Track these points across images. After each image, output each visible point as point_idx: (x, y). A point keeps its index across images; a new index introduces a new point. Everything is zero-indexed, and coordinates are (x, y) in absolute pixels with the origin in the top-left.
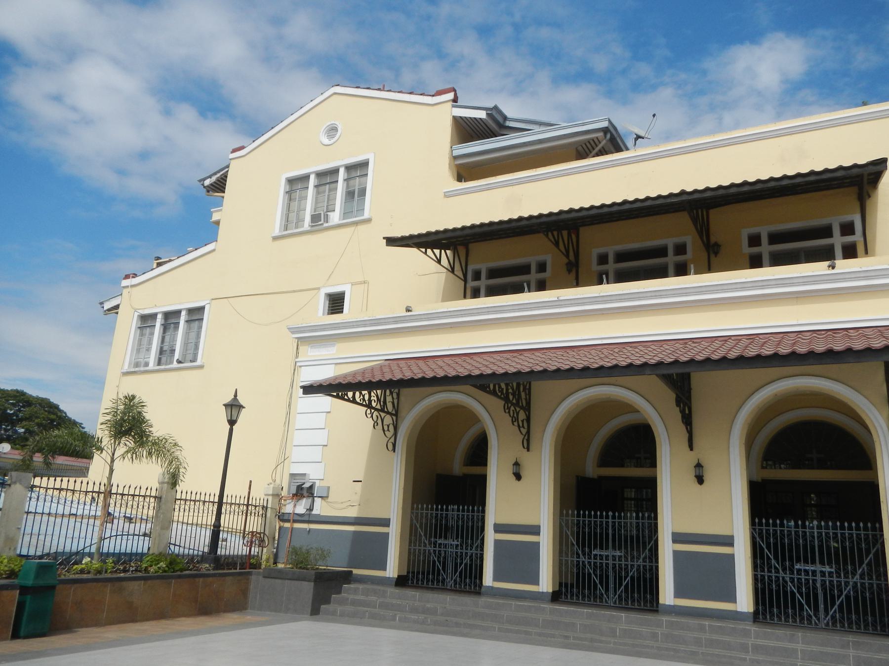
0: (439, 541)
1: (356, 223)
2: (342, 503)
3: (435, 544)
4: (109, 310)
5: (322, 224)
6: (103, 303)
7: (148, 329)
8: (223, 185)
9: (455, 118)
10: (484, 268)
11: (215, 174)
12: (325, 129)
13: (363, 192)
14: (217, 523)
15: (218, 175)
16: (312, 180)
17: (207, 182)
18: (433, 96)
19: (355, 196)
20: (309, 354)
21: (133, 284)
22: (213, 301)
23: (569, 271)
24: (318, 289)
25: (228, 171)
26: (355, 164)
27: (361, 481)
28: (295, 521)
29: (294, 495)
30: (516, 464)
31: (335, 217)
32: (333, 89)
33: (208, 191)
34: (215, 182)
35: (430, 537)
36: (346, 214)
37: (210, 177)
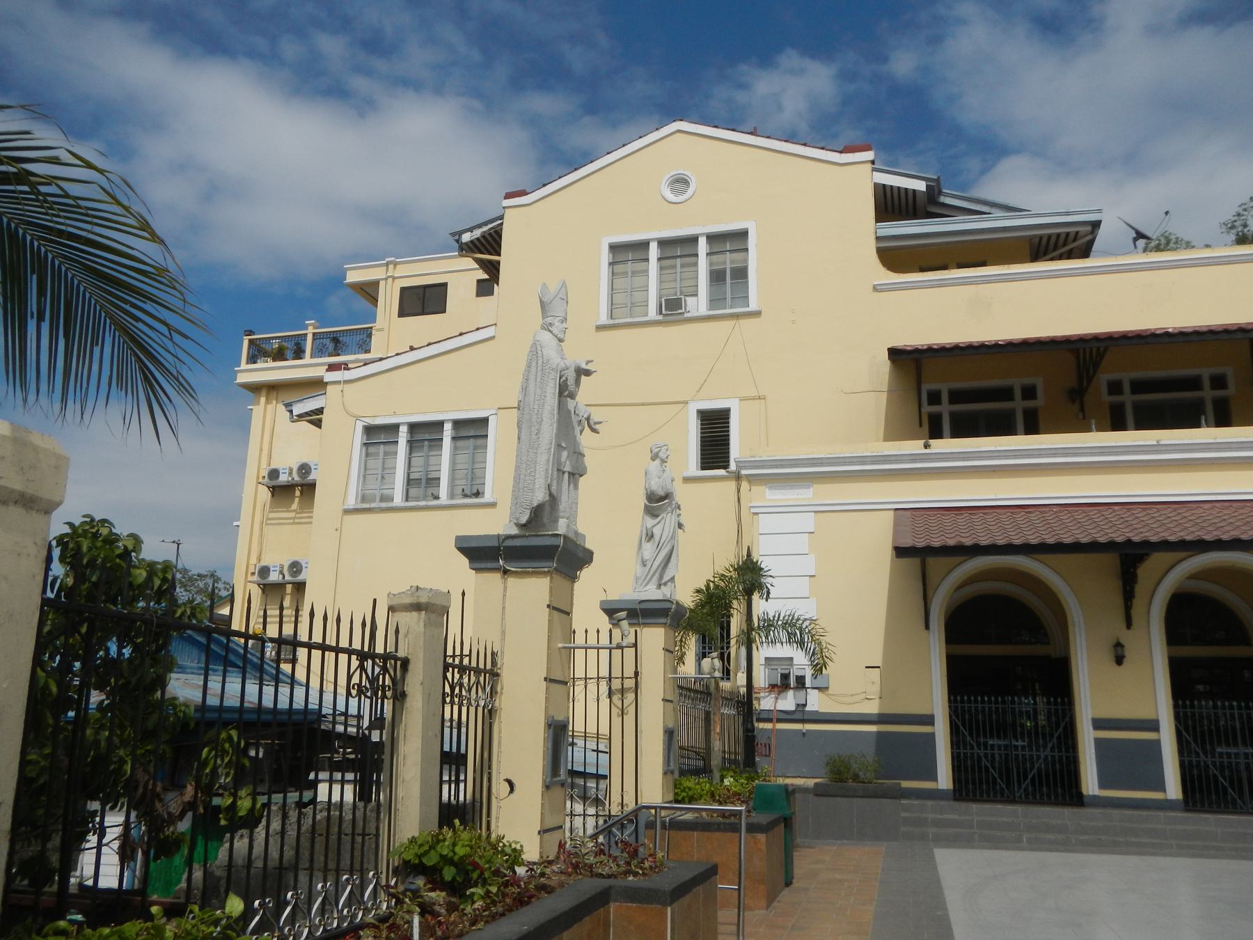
0: (991, 742)
1: (737, 316)
2: (852, 695)
3: (985, 744)
4: (300, 416)
6: (291, 405)
7: (382, 446)
9: (876, 185)
10: (944, 388)
13: (741, 274)
15: (485, 229)
17: (466, 238)
18: (841, 152)
22: (500, 411)
23: (1073, 401)
24: (686, 403)
25: (503, 223)
27: (879, 667)
28: (780, 721)
29: (773, 687)
30: (1118, 645)
31: (699, 304)
34: (478, 239)
35: (978, 735)
36: (714, 301)
37: (471, 230)
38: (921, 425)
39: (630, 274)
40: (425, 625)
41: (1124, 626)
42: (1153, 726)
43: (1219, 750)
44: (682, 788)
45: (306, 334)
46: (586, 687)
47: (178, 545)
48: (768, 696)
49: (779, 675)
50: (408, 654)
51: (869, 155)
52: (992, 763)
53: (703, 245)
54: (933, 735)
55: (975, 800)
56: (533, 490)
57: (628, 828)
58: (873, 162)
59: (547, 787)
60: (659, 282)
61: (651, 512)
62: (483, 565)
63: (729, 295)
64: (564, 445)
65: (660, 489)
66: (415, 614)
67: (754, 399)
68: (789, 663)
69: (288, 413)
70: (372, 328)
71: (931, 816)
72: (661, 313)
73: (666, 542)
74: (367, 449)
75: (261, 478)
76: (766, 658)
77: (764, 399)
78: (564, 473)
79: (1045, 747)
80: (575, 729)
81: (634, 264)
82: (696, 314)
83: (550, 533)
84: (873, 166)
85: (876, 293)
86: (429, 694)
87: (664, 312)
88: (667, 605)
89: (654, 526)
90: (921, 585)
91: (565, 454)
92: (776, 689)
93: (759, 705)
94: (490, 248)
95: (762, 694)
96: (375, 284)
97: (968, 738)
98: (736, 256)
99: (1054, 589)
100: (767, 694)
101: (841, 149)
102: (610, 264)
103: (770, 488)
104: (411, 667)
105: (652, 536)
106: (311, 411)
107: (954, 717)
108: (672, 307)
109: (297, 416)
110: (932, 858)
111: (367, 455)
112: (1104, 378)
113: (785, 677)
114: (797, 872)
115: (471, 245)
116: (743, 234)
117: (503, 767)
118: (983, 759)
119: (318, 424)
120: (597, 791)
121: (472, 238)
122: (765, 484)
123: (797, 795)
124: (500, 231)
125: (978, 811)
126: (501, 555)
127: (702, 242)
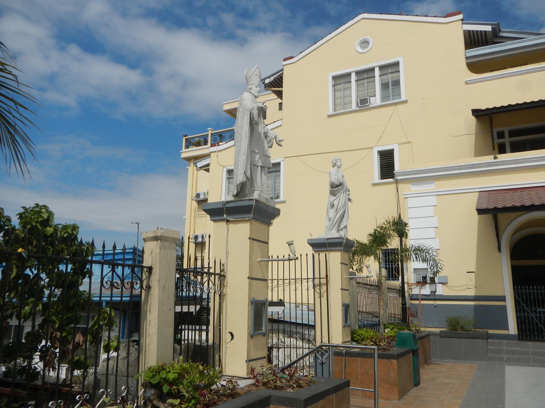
0: (539, 310)
1: (395, 104)
2: (460, 287)
3: (536, 311)
4: (200, 168)
5: (369, 105)
6: (196, 163)
8: (280, 82)
9: (464, 31)
11: (273, 75)
12: (359, 42)
13: (397, 83)
14: (404, 302)
15: (275, 76)
16: (353, 77)
17: (267, 81)
18: (445, 17)
20: (412, 189)
21: (219, 149)
22: (286, 159)
24: (372, 148)
26: (386, 65)
27: (474, 272)
28: (422, 300)
29: (418, 283)
31: (376, 100)
32: (361, 15)
33: (265, 87)
34: (272, 81)
36: (384, 98)
37: (269, 77)
38: (494, 150)
39: (342, 90)
40: (160, 248)
44: (358, 334)
45: (208, 134)
46: (301, 283)
47: (138, 224)
48: (416, 287)
49: (421, 277)
50: (152, 265)
51: (461, 16)
53: (377, 72)
54: (505, 307)
55: (530, 340)
57: (325, 355)
58: (462, 20)
59: (251, 336)
60: (356, 92)
61: (333, 193)
62: (216, 218)
63: (391, 95)
64: (257, 151)
65: (336, 181)
66: (155, 242)
67: (406, 143)
68: (426, 271)
69: (195, 167)
70: (234, 129)
71: (505, 348)
72: (358, 106)
73: (341, 208)
74: (229, 180)
75: (193, 197)
76: (414, 269)
77: (411, 143)
78: (258, 166)
80: (309, 303)
81: (344, 85)
83: (248, 198)
84: (463, 22)
85: (467, 85)
86: (164, 287)
87: (359, 105)
88: (341, 240)
89: (334, 200)
91: (257, 156)
92: (420, 284)
93: (412, 292)
94: (279, 85)
95: (413, 287)
96: (235, 110)
97: (526, 308)
98: (394, 75)
100: (415, 286)
101: (445, 16)
102: (333, 86)
103: (413, 185)
104: (153, 272)
105: (334, 206)
106: (205, 165)
107: (517, 297)
108: (363, 103)
109: (199, 168)
110: (503, 371)
111: (229, 183)
113: (425, 278)
115: (270, 85)
116: (397, 64)
117: (229, 324)
118: (535, 319)
119: (208, 170)
120: (309, 336)
121: (270, 81)
122: (410, 183)
123: (431, 337)
124: (282, 77)
125: (531, 346)
126: (224, 212)
127: (377, 70)
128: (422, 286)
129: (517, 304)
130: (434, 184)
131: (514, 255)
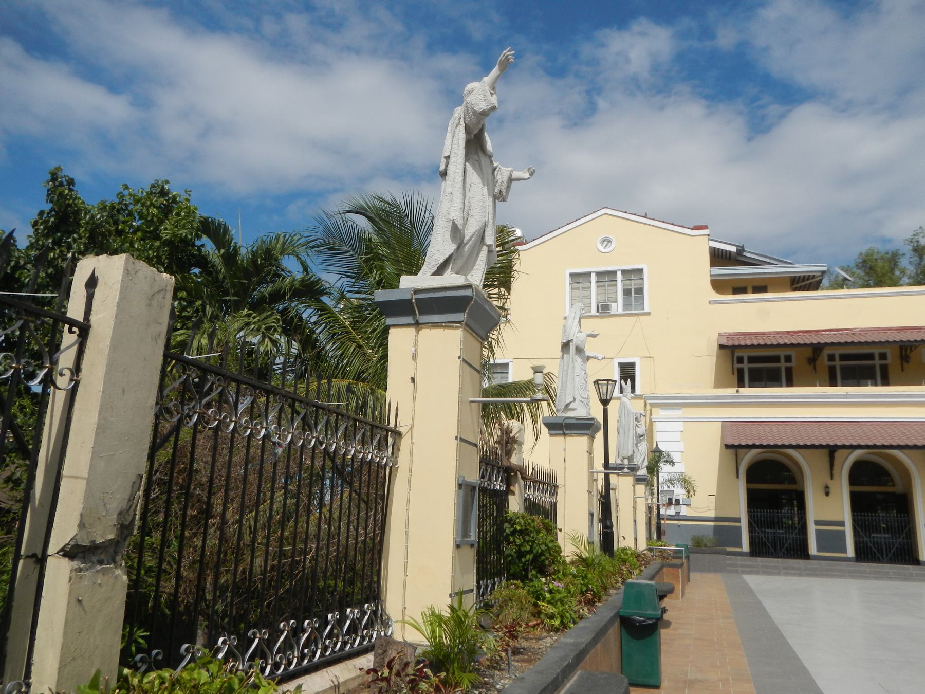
0: (767, 531)
1: (638, 314)
3: (765, 532)
9: (711, 248)
13: (640, 291)
16: (593, 278)
18: (692, 229)
19: (634, 294)
23: (810, 364)
28: (668, 519)
30: (827, 487)
31: (617, 307)
36: (627, 306)
38: (733, 374)
41: (829, 478)
42: (842, 524)
43: (873, 535)
52: (768, 540)
54: (740, 528)
55: (759, 556)
56: (628, 450)
71: (740, 563)
72: (598, 311)
79: (792, 533)
82: (617, 313)
88: (646, 477)
90: (735, 457)
99: (796, 459)
101: (692, 227)
102: (570, 284)
108: (604, 309)
112: (826, 352)
113: (670, 499)
114: (691, 578)
116: (641, 271)
125: (760, 561)
127: (619, 274)
128: (667, 507)
129: (750, 525)
130: (681, 410)
131: (749, 481)
